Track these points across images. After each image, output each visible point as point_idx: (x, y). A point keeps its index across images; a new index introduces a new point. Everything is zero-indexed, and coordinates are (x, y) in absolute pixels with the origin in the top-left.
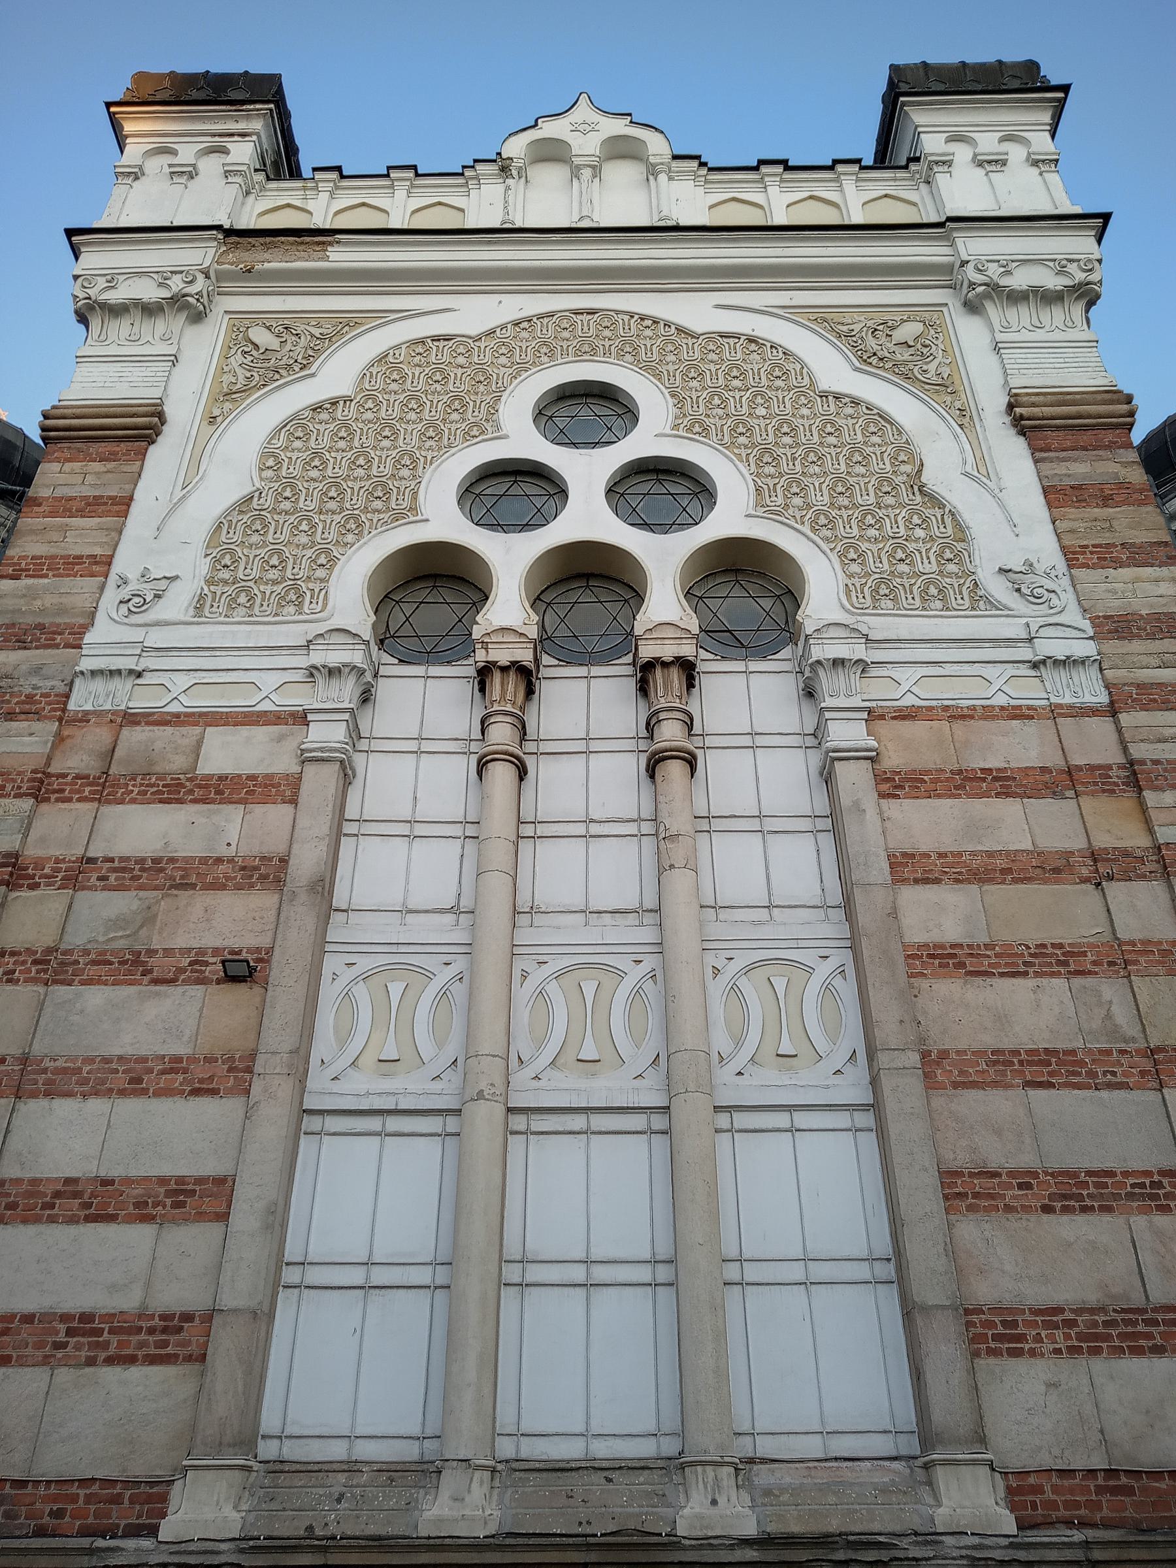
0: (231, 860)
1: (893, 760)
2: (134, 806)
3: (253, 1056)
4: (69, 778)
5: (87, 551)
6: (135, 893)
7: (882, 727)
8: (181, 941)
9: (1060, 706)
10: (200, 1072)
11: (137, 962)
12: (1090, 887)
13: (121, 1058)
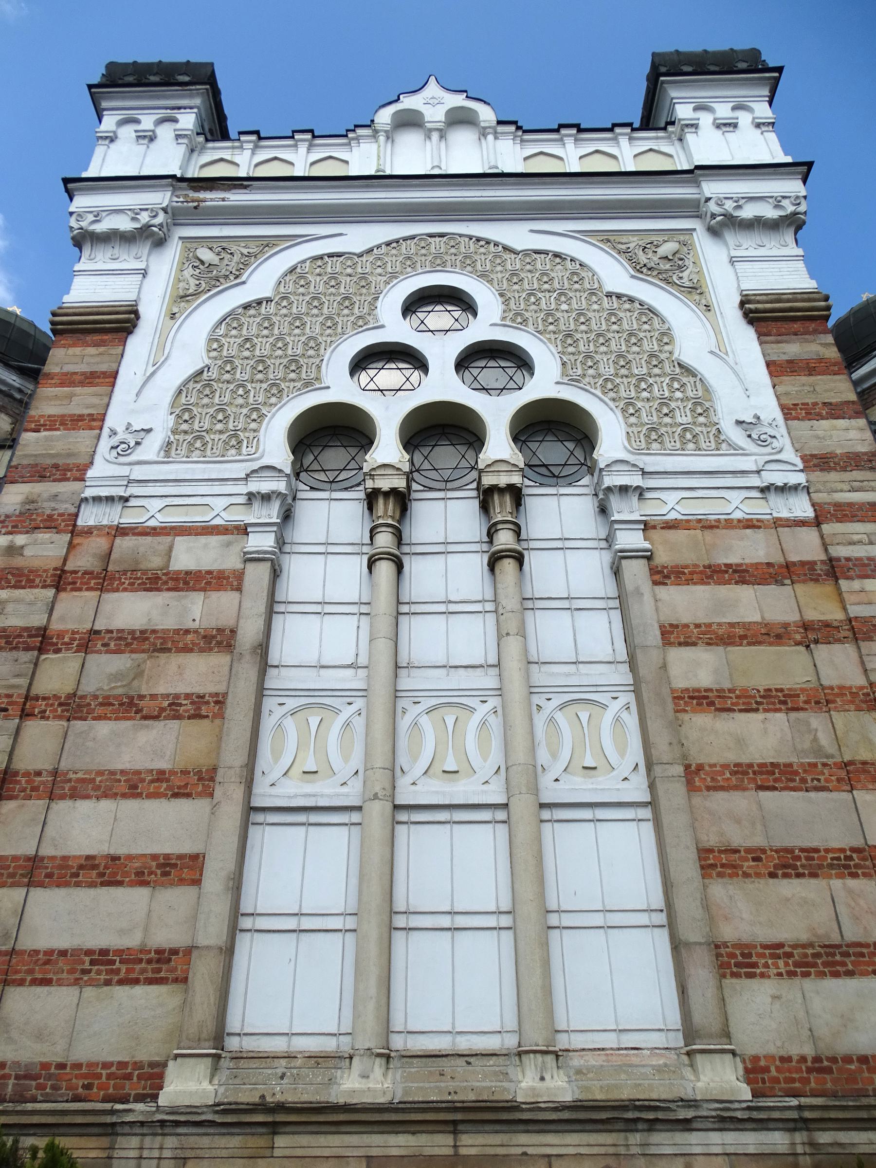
0: (196, 631)
1: (663, 558)
2: (126, 594)
3: (215, 769)
4: (80, 574)
5: (86, 412)
6: (127, 655)
7: (655, 534)
8: (161, 689)
9: (780, 519)
10: (177, 781)
11: (131, 704)
12: (802, 649)
13: (122, 772)
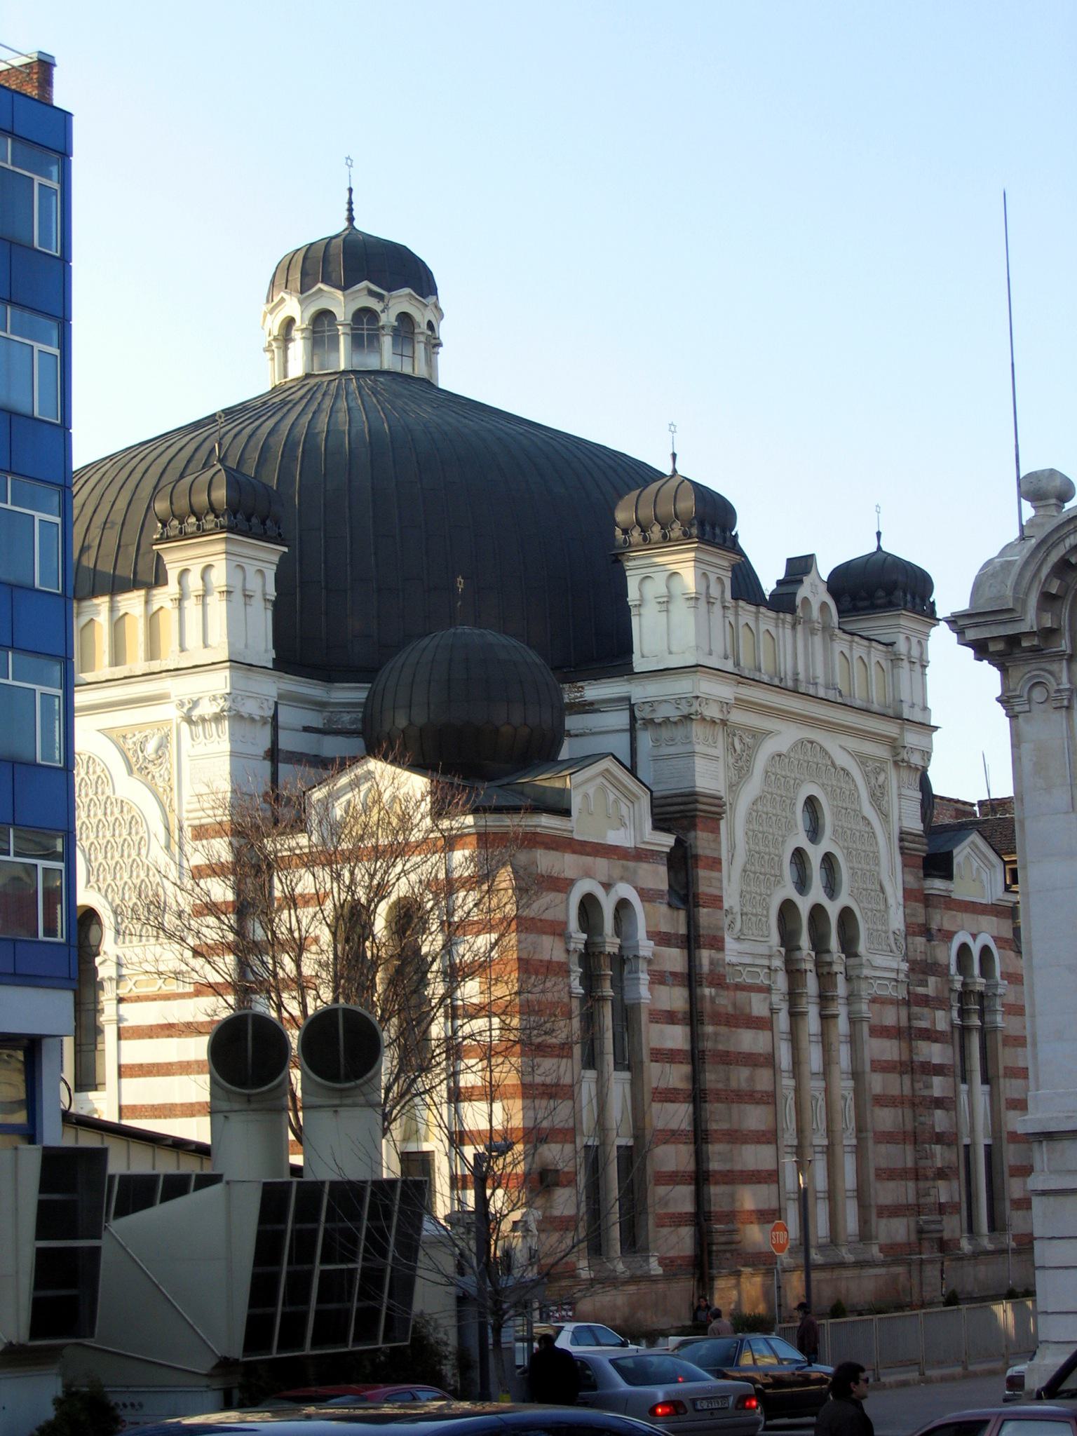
1: (872, 1022)
8: (758, 1088)
